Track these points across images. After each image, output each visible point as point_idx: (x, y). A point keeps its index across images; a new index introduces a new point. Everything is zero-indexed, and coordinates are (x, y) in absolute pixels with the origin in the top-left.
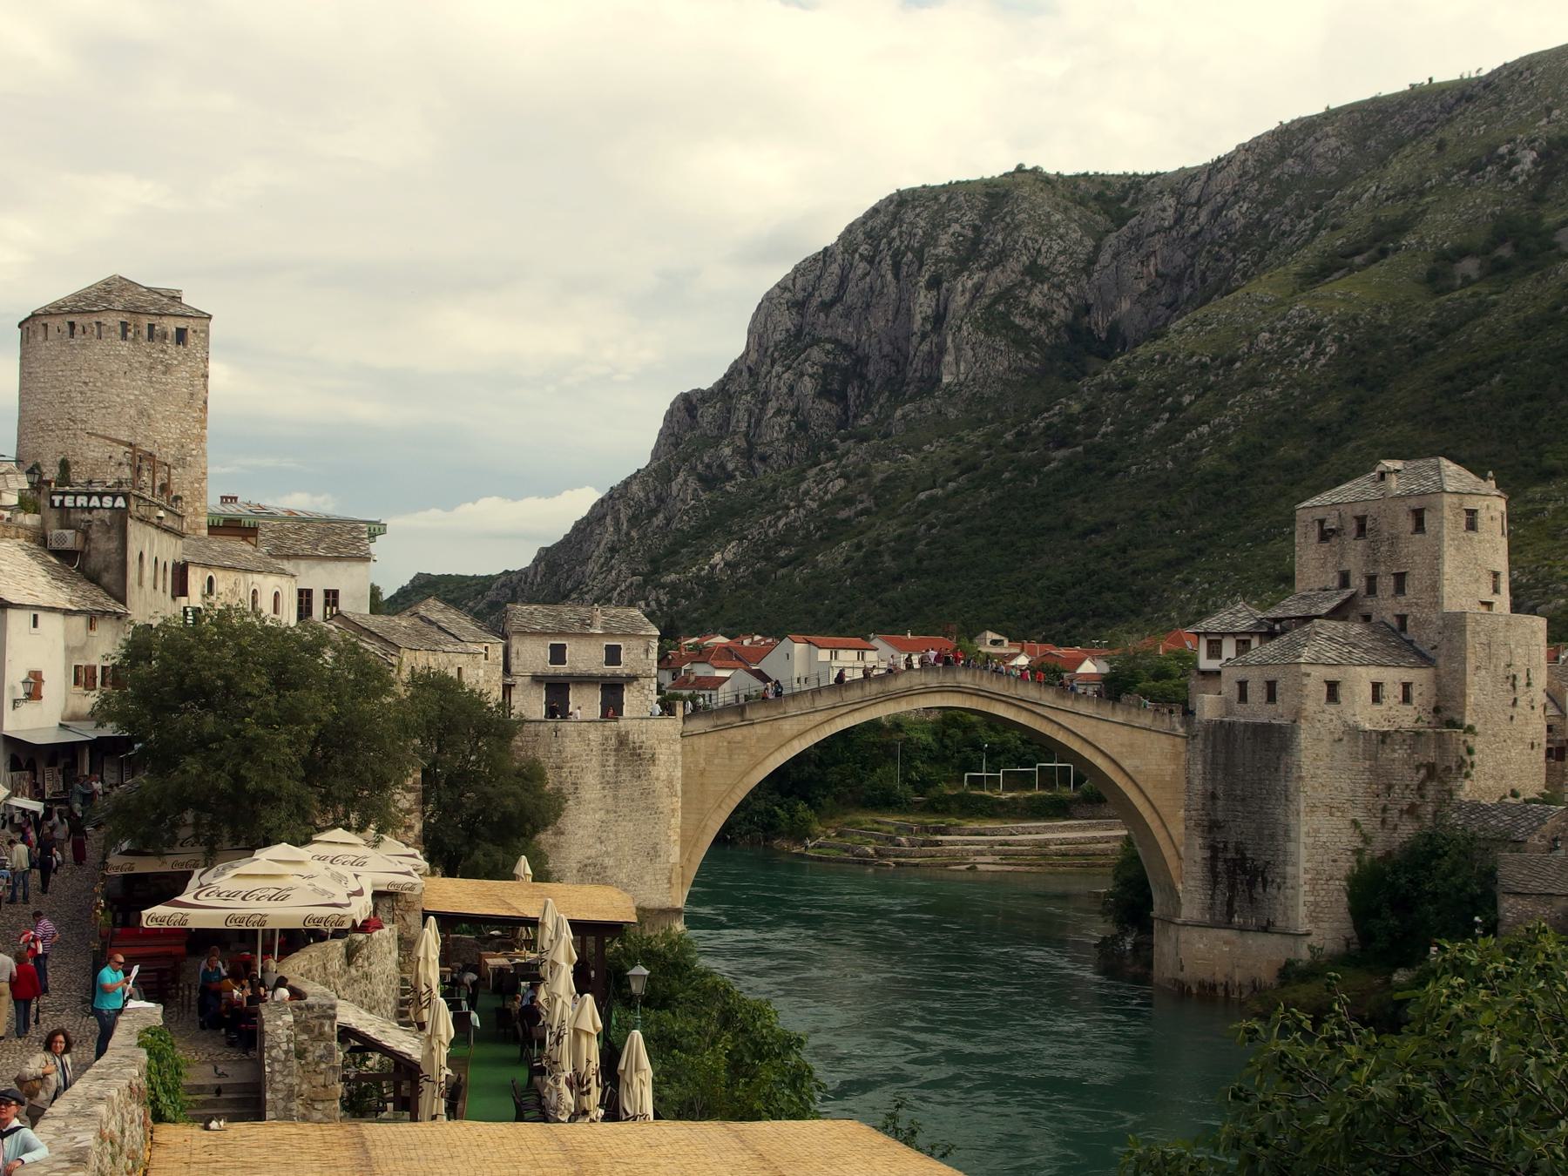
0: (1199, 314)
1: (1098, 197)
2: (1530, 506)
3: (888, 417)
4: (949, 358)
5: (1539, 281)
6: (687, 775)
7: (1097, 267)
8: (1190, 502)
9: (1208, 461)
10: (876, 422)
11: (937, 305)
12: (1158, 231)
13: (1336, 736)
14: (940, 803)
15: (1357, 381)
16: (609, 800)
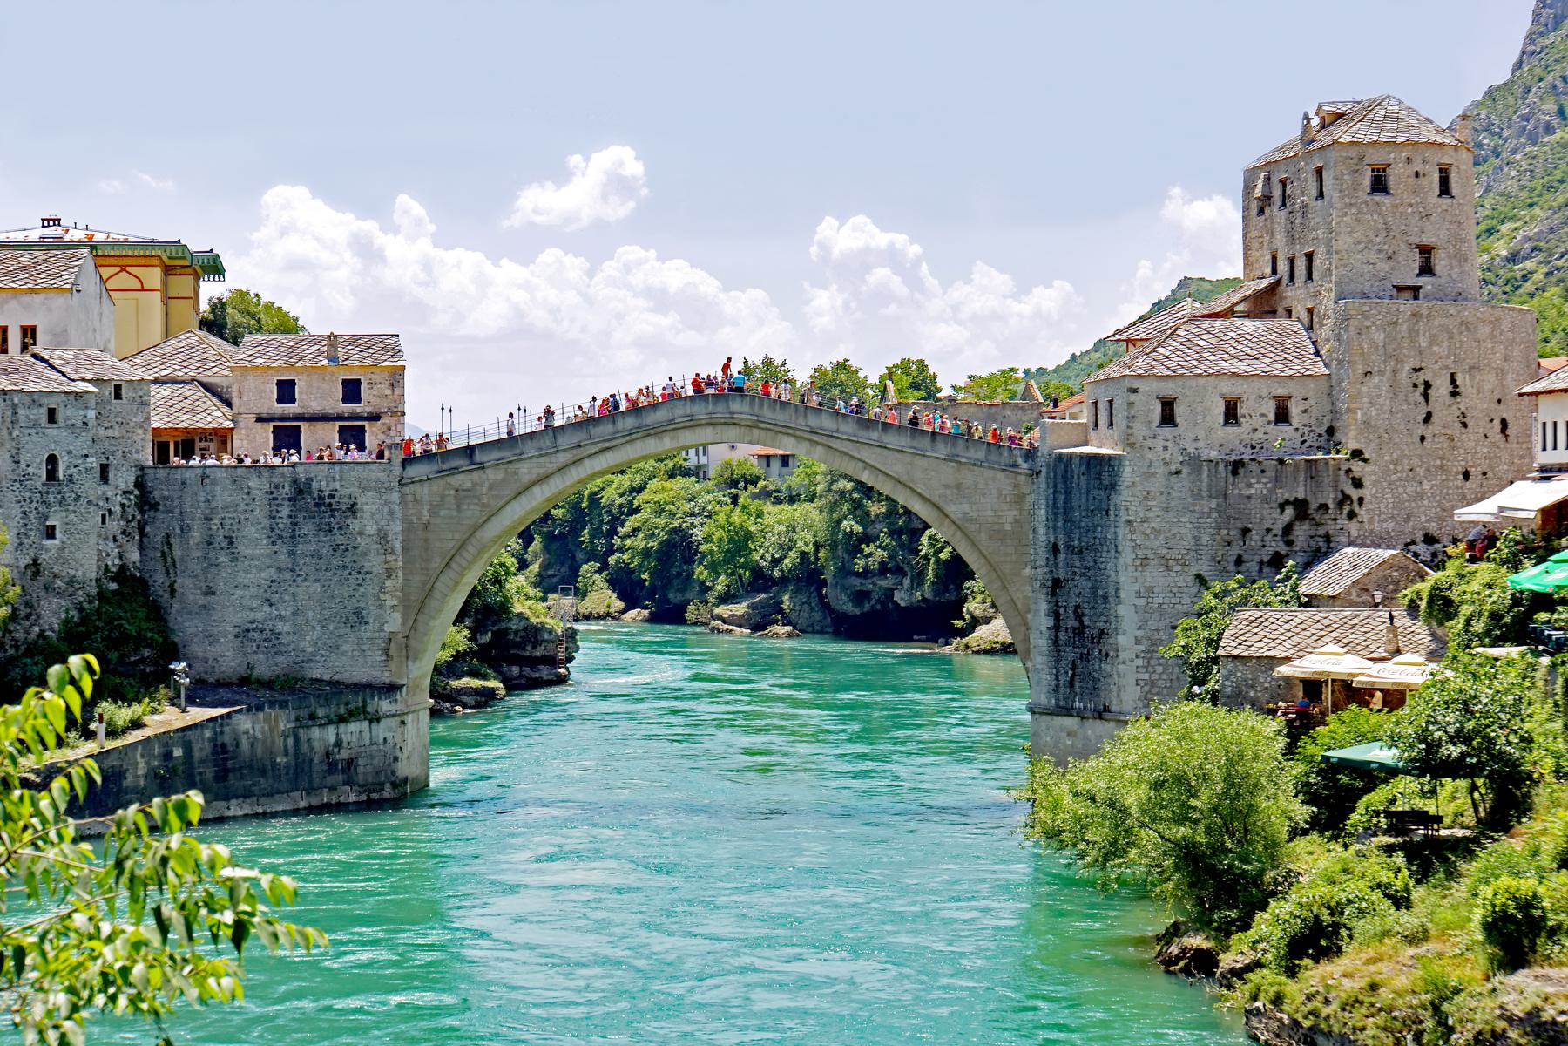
6: (408, 528)
13: (1173, 468)
16: (283, 557)
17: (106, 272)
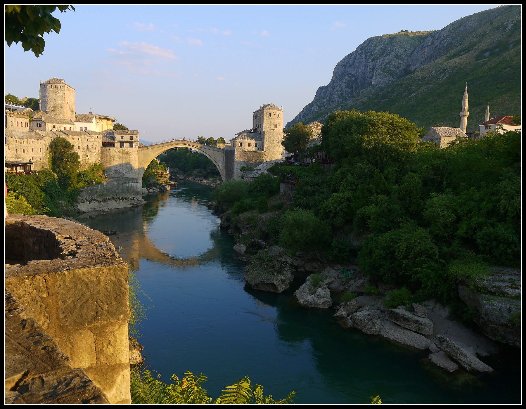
4: (374, 78)
11: (374, 65)
17: (98, 120)
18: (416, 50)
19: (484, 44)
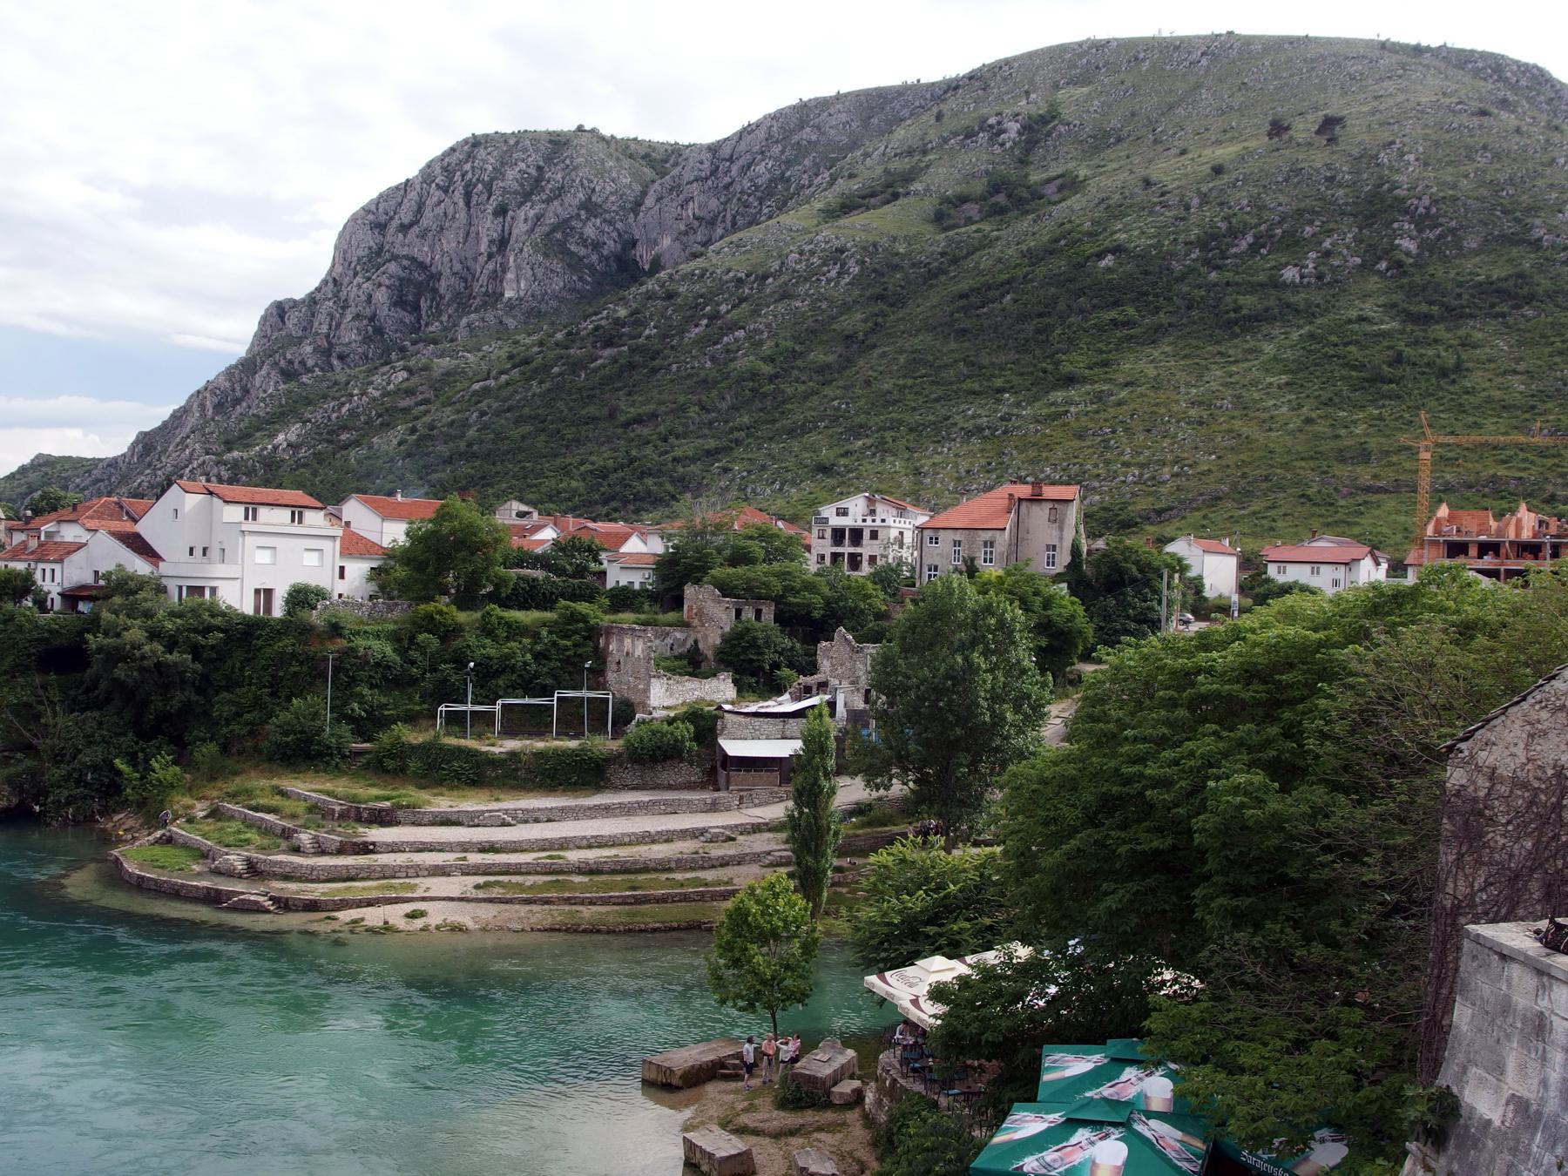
0: (735, 238)
1: (646, 157)
2: (1053, 409)
3: (455, 325)
4: (510, 276)
5: (1035, 221)
7: (643, 208)
8: (728, 397)
9: (744, 362)
10: (445, 329)
11: (503, 231)
12: (697, 180)
14: (391, 756)
15: (880, 298)
18: (652, 192)
19: (943, 177)
